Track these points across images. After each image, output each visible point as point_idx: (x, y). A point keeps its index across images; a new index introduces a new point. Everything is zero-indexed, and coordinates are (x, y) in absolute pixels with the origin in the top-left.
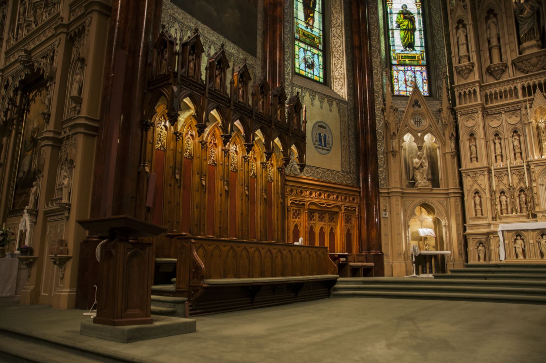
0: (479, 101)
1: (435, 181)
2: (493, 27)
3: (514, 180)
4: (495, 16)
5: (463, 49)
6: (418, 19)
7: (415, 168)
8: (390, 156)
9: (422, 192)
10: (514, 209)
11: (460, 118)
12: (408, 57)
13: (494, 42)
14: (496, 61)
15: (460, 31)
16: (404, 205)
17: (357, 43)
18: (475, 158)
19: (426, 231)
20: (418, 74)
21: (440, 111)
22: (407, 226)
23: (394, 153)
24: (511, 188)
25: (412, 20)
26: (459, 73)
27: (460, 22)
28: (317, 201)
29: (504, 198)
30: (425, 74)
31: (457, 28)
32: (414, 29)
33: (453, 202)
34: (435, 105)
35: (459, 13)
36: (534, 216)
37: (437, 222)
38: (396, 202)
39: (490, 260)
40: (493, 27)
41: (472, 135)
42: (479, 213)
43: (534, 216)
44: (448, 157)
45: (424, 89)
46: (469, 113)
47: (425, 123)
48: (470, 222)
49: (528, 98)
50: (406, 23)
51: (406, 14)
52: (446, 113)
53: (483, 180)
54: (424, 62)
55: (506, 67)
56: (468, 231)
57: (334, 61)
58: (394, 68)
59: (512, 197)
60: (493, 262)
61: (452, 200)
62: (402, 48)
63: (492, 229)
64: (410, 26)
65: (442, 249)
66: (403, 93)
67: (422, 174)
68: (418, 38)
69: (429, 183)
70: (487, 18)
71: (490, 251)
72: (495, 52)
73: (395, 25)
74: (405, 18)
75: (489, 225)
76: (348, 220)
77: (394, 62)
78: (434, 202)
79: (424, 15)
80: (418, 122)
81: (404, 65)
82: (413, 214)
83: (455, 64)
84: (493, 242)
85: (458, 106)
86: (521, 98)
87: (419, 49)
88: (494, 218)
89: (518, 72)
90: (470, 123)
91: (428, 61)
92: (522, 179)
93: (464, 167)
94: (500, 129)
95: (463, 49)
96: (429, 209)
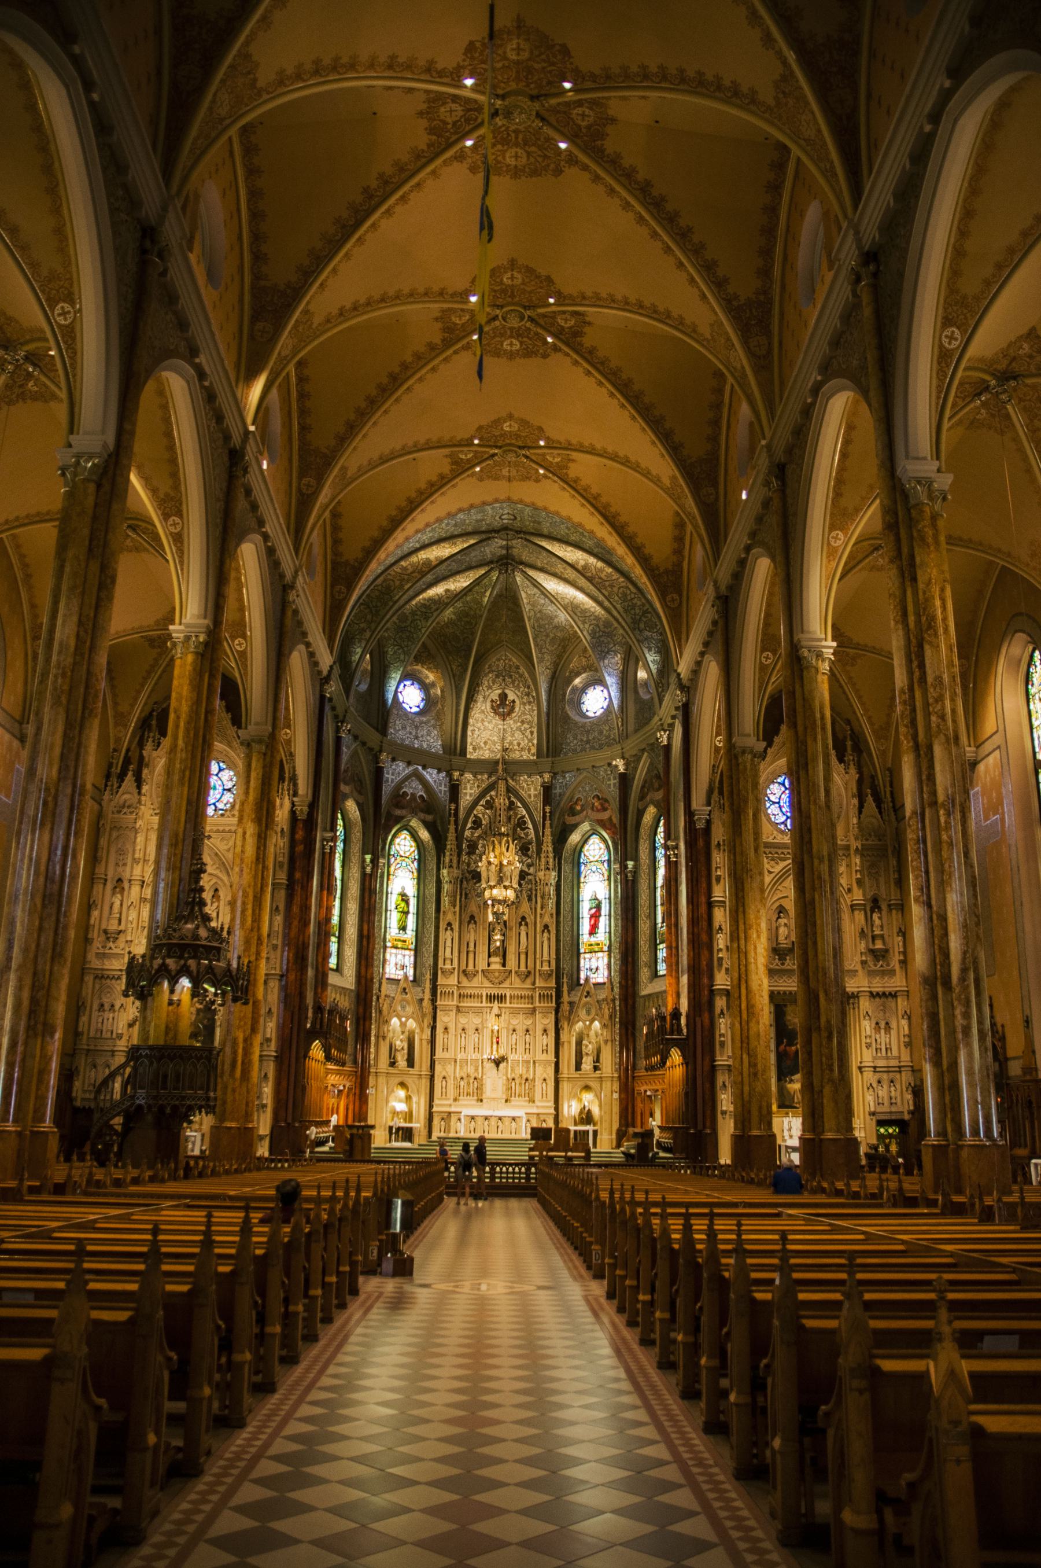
0: (455, 1003)
1: (411, 1063)
2: (472, 931)
3: (470, 1070)
4: (475, 923)
5: (448, 950)
6: (413, 902)
7: (396, 1050)
8: (381, 1039)
9: (402, 1073)
10: (468, 1094)
11: (439, 1013)
12: (400, 940)
13: (472, 945)
14: (471, 967)
15: (449, 932)
16: (387, 1083)
17: (365, 932)
18: (445, 1049)
19: (401, 1107)
20: (407, 957)
21: (421, 1000)
22: (387, 1101)
23: (384, 1038)
24: (468, 1076)
25: (407, 902)
26: (442, 972)
27: (449, 924)
28: (334, 1082)
29: (462, 1083)
30: (412, 959)
31: (446, 929)
32: (407, 913)
33: (425, 1083)
34: (415, 992)
35: (450, 917)
36: (481, 1101)
37: (408, 1098)
38: (382, 1080)
39: (449, 1132)
40: (472, 931)
41: (446, 1029)
42: (444, 1094)
43: (481, 1101)
44: (424, 1043)
45: (411, 972)
46: (446, 1011)
47: (409, 1009)
48: (436, 1101)
49: (489, 1005)
50: (403, 904)
51: (404, 898)
52: (427, 1003)
53: (450, 1068)
54: (413, 947)
55: (477, 972)
56: (435, 1109)
57: (346, 948)
58: (388, 950)
59: (469, 1083)
60: (452, 1135)
61: (424, 1081)
62: (397, 931)
63: (453, 1109)
64: (406, 909)
65: (411, 1121)
66: (392, 977)
67: (403, 1056)
68: (411, 921)
69: (406, 1063)
70: (469, 922)
71: (449, 1126)
72: (471, 956)
73: (394, 906)
74: (403, 900)
75: (450, 1105)
76: (348, 1096)
77: (389, 944)
78: (409, 1081)
79: (418, 897)
80: (403, 1007)
81: (396, 948)
82: (393, 1091)
83: (440, 964)
84: (454, 1118)
85: (438, 1002)
86: (484, 1004)
87: (410, 935)
88: (455, 1100)
89: (485, 981)
90: (446, 1019)
91: (416, 946)
92: (476, 1070)
93: (437, 1056)
94: (466, 1026)
95: (448, 950)
96: (403, 1085)
